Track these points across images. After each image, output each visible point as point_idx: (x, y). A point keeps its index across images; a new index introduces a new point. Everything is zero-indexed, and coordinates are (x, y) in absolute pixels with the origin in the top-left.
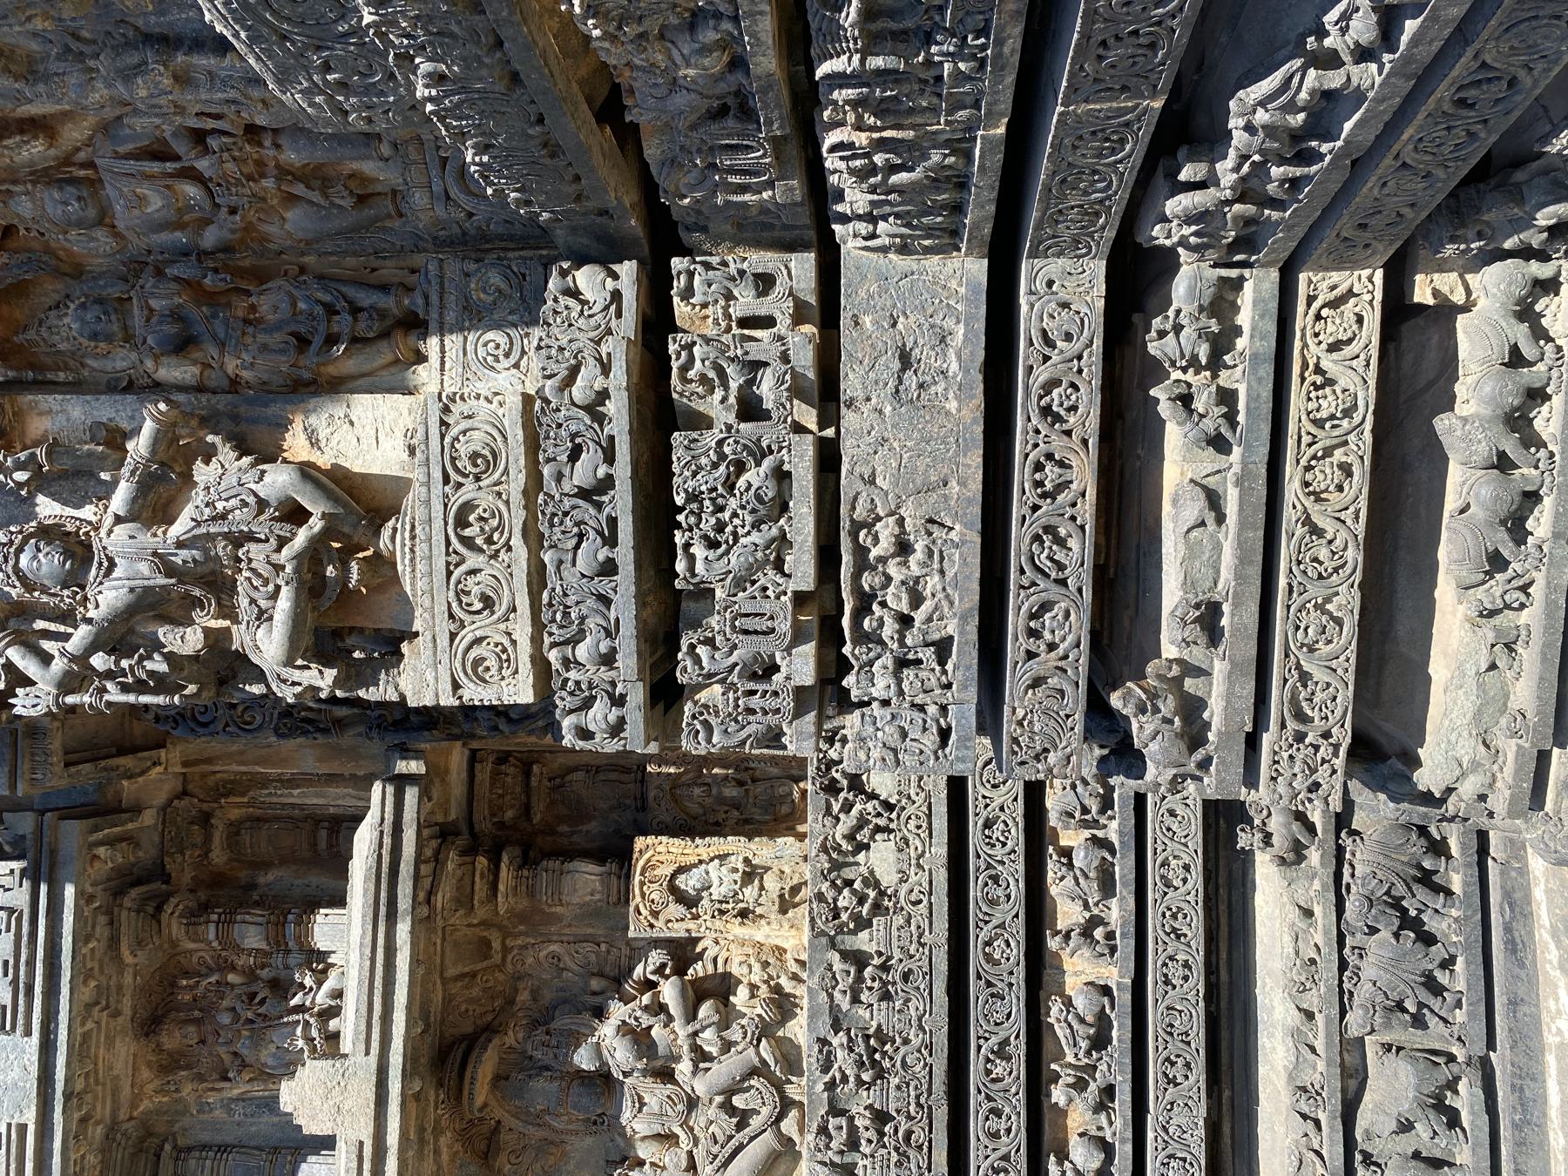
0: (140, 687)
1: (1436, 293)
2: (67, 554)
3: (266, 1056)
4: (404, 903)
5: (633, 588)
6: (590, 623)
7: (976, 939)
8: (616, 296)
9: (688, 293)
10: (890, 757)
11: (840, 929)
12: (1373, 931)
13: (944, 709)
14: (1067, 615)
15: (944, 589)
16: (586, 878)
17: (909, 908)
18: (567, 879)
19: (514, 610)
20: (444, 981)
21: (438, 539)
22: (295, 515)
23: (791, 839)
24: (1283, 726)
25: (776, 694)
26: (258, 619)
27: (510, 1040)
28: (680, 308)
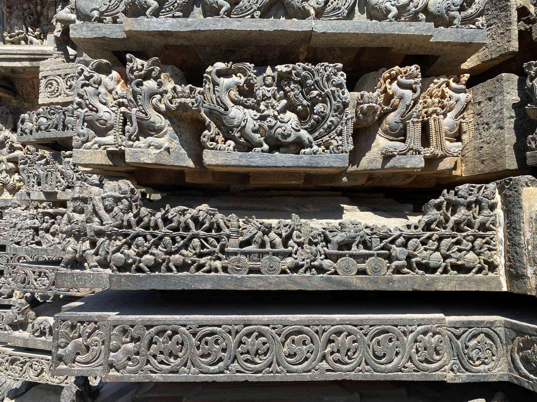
3: (14, 21)
5: (59, 136)
6: (50, 122)
10: (12, 225)
14: (45, 285)
15: (54, 244)
19: (67, 96)
20: (32, 78)
24: (10, 356)
25: (33, 186)
26: (72, 8)
27: (13, 101)
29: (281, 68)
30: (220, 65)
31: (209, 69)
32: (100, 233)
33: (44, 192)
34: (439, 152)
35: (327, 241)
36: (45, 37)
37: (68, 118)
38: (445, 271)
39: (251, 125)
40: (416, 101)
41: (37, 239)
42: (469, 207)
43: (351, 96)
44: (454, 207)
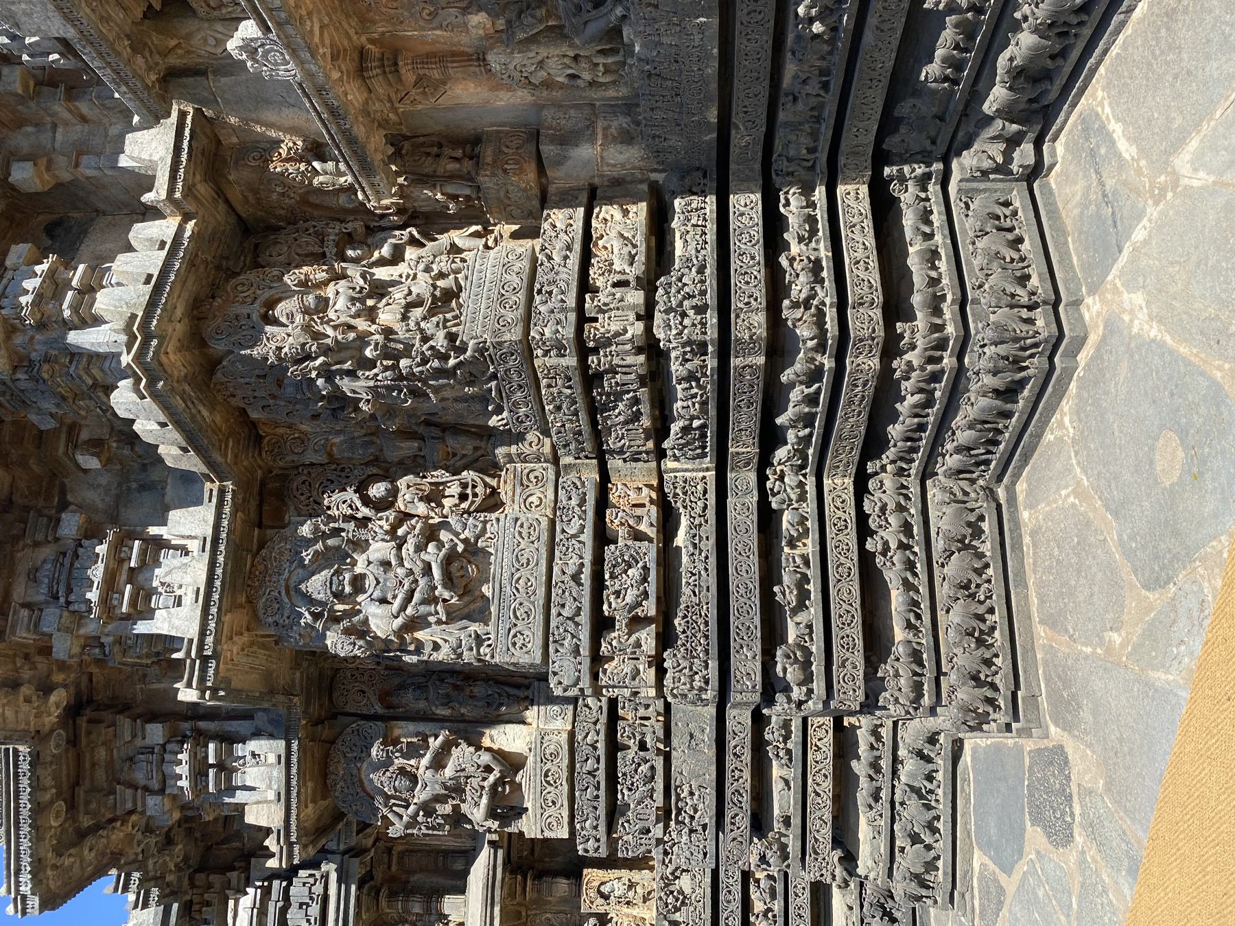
0: (433, 828)
1: (849, 724)
2: (411, 781)
4: (497, 899)
6: (590, 815)
7: (723, 915)
8: (601, 707)
9: (624, 708)
11: (668, 912)
12: (874, 917)
13: (705, 847)
16: (562, 886)
17: (695, 903)
18: (554, 885)
21: (538, 781)
22: (488, 769)
23: (647, 871)
28: (621, 712)
29: (607, 576)
30: (605, 607)
31: (606, 614)
32: (691, 669)
33: (656, 823)
34: (648, 499)
35: (693, 554)
36: (446, 916)
37: (588, 796)
38: (706, 499)
39: (636, 592)
40: (624, 511)
41: (700, 828)
42: (676, 488)
43: (621, 543)
44: (676, 495)
